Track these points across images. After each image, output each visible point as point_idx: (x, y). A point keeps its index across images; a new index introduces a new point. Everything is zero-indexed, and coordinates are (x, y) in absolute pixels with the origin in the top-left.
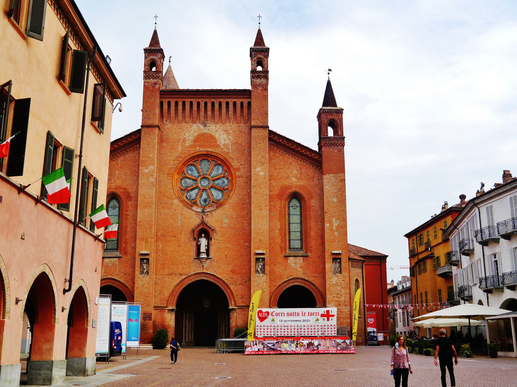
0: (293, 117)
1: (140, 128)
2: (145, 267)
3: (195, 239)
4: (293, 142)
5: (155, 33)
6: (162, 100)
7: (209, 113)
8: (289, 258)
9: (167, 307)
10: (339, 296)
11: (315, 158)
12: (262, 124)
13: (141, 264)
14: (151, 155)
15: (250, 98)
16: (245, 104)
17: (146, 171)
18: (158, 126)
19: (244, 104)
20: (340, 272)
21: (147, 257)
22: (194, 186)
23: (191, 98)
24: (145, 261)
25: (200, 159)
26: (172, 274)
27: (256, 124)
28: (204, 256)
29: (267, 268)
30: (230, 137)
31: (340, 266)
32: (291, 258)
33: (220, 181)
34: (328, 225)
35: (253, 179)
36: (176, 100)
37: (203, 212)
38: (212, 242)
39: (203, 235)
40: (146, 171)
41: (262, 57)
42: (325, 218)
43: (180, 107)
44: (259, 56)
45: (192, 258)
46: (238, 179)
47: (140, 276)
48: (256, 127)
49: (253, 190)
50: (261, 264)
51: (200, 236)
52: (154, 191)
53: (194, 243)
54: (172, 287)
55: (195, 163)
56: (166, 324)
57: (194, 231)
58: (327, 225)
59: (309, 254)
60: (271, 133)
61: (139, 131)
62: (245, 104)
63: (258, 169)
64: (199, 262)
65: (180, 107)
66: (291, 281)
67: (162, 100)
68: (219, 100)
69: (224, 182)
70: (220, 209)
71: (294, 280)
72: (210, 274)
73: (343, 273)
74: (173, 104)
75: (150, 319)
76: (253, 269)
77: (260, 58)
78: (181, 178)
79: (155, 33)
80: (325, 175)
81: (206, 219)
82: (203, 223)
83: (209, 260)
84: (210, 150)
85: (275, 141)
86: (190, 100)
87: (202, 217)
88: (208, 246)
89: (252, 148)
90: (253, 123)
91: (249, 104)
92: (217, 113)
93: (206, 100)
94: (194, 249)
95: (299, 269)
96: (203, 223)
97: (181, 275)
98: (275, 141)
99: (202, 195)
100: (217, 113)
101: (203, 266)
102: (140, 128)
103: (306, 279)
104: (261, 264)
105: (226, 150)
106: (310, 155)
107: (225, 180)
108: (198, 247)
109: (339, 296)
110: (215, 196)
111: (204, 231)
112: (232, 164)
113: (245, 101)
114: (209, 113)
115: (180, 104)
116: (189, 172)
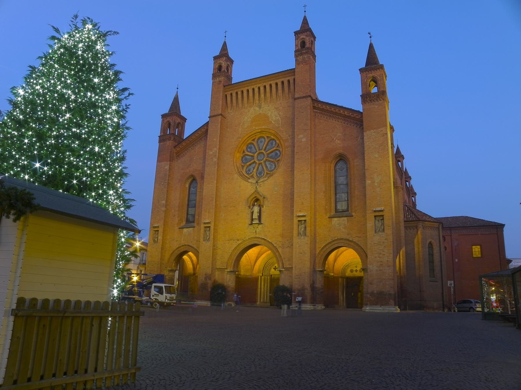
0: (338, 85)
1: (208, 119)
2: (208, 234)
3: (249, 207)
4: (336, 106)
5: (225, 44)
6: (226, 93)
7: (262, 96)
8: (333, 219)
9: (226, 269)
10: (381, 256)
11: (357, 117)
12: (304, 95)
13: (205, 231)
14: (215, 140)
15: (294, 75)
16: (292, 82)
17: (211, 153)
18: (221, 115)
19: (294, 84)
20: (384, 230)
21: (208, 225)
22: (252, 161)
23: (247, 87)
24: (208, 229)
25: (257, 137)
26: (231, 240)
27: (299, 96)
28: (257, 221)
29: (308, 229)
30: (280, 113)
31: (383, 224)
32: (336, 219)
33: (273, 154)
34: (370, 182)
35: (296, 146)
36: (236, 91)
37: (257, 182)
38: (263, 209)
39: (256, 203)
40: (211, 153)
41: (304, 37)
42: (366, 175)
43: (240, 96)
44: (302, 37)
45: (247, 225)
46: (286, 149)
47: (204, 242)
48: (298, 98)
49: (296, 157)
50: (303, 225)
51: (254, 205)
52: (216, 169)
53: (249, 211)
54: (231, 251)
55: (252, 142)
56: (225, 284)
57: (248, 200)
58: (368, 182)
59: (353, 214)
60: (316, 101)
61: (207, 123)
62: (292, 82)
63: (301, 136)
64: (252, 228)
65: (240, 96)
66: (336, 242)
67: (226, 93)
68: (269, 83)
69: (277, 154)
70: (271, 178)
71: (339, 241)
72: (262, 239)
73: (385, 231)
74: (234, 95)
75: (210, 279)
76: (295, 232)
77: (303, 38)
78: (242, 156)
79: (225, 44)
80: (366, 131)
81: (259, 189)
82: (256, 191)
83: (261, 226)
84: (263, 127)
85: (318, 109)
86: (247, 88)
87: (256, 188)
88: (260, 212)
89: (296, 118)
90: (296, 96)
91: (294, 79)
92: (268, 94)
93: (259, 85)
94: (249, 216)
95: (344, 230)
96: (256, 191)
97: (238, 240)
98: (318, 109)
99: (258, 168)
100: (268, 94)
101: (256, 232)
102: (208, 119)
103: (351, 239)
104: (303, 225)
105: (277, 125)
106: (352, 116)
107: (278, 152)
108: (252, 213)
109: (381, 256)
110: (269, 168)
111: (256, 200)
112: (282, 136)
113: (291, 79)
114: (262, 96)
115: (239, 93)
116: (249, 150)
